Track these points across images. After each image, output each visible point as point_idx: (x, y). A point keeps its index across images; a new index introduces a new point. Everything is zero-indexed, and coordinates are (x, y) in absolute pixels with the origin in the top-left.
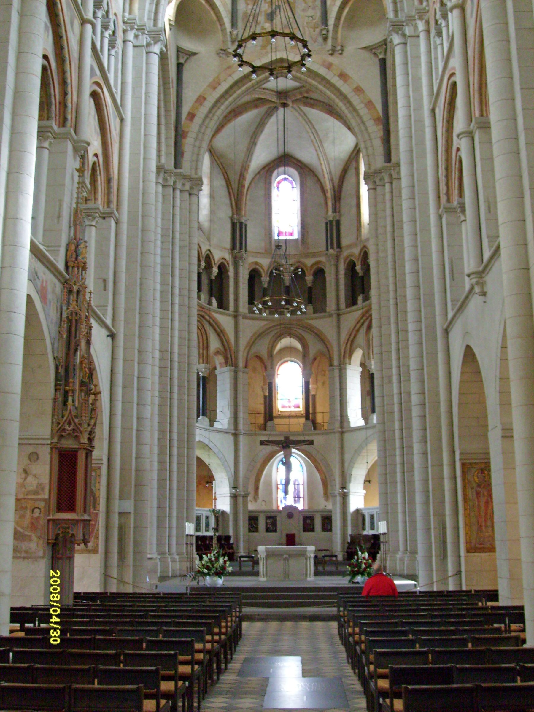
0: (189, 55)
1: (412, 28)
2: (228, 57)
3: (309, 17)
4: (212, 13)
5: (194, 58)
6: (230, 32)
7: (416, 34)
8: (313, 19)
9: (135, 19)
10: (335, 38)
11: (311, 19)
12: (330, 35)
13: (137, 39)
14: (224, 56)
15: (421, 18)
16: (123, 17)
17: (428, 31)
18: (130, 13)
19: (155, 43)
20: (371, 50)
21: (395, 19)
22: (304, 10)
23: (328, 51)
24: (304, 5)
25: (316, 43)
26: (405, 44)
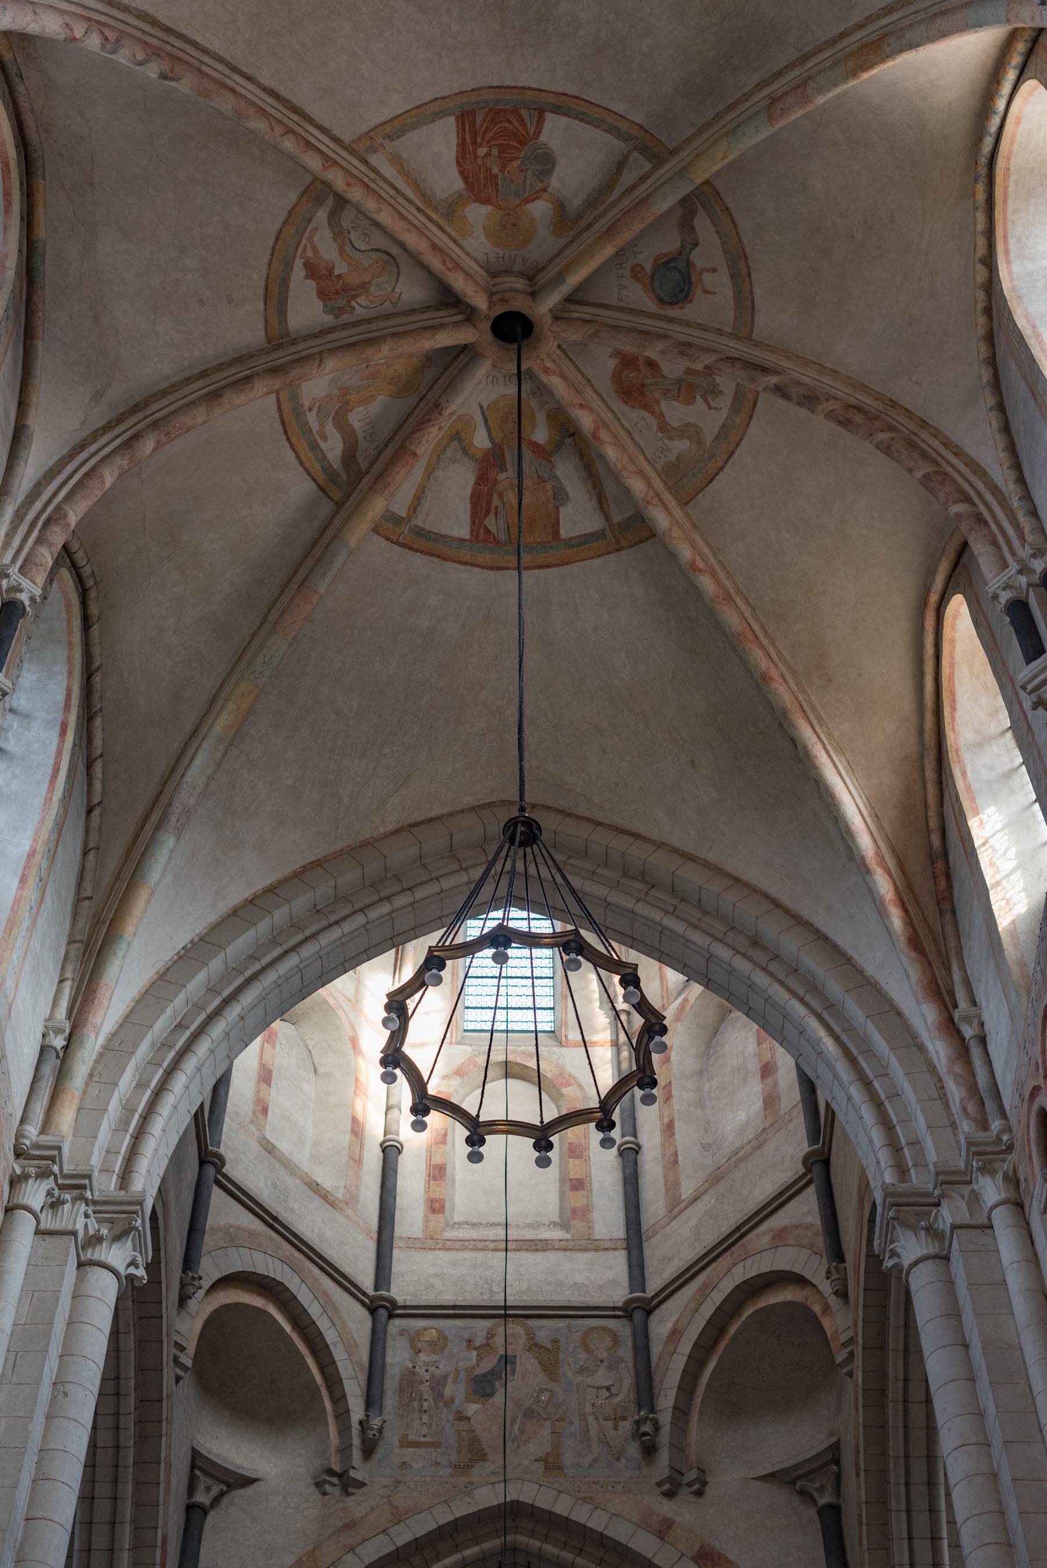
0: (228, 1485)
1: (963, 1205)
2: (348, 1494)
3: (598, 1388)
4: (310, 1361)
5: (239, 1494)
6: (361, 1423)
7: (982, 1219)
8: (611, 1395)
9: (59, 1148)
10: (678, 1448)
11: (605, 1393)
12: (664, 1437)
13: (55, 1214)
14: (336, 1491)
15: (987, 1170)
16: (19, 1135)
17: (1019, 1206)
18: (45, 1128)
19: (117, 1238)
20: (793, 1483)
21: (902, 1187)
22: (582, 1371)
23: (659, 1484)
24: (583, 1356)
25: (623, 1461)
26: (945, 1258)
